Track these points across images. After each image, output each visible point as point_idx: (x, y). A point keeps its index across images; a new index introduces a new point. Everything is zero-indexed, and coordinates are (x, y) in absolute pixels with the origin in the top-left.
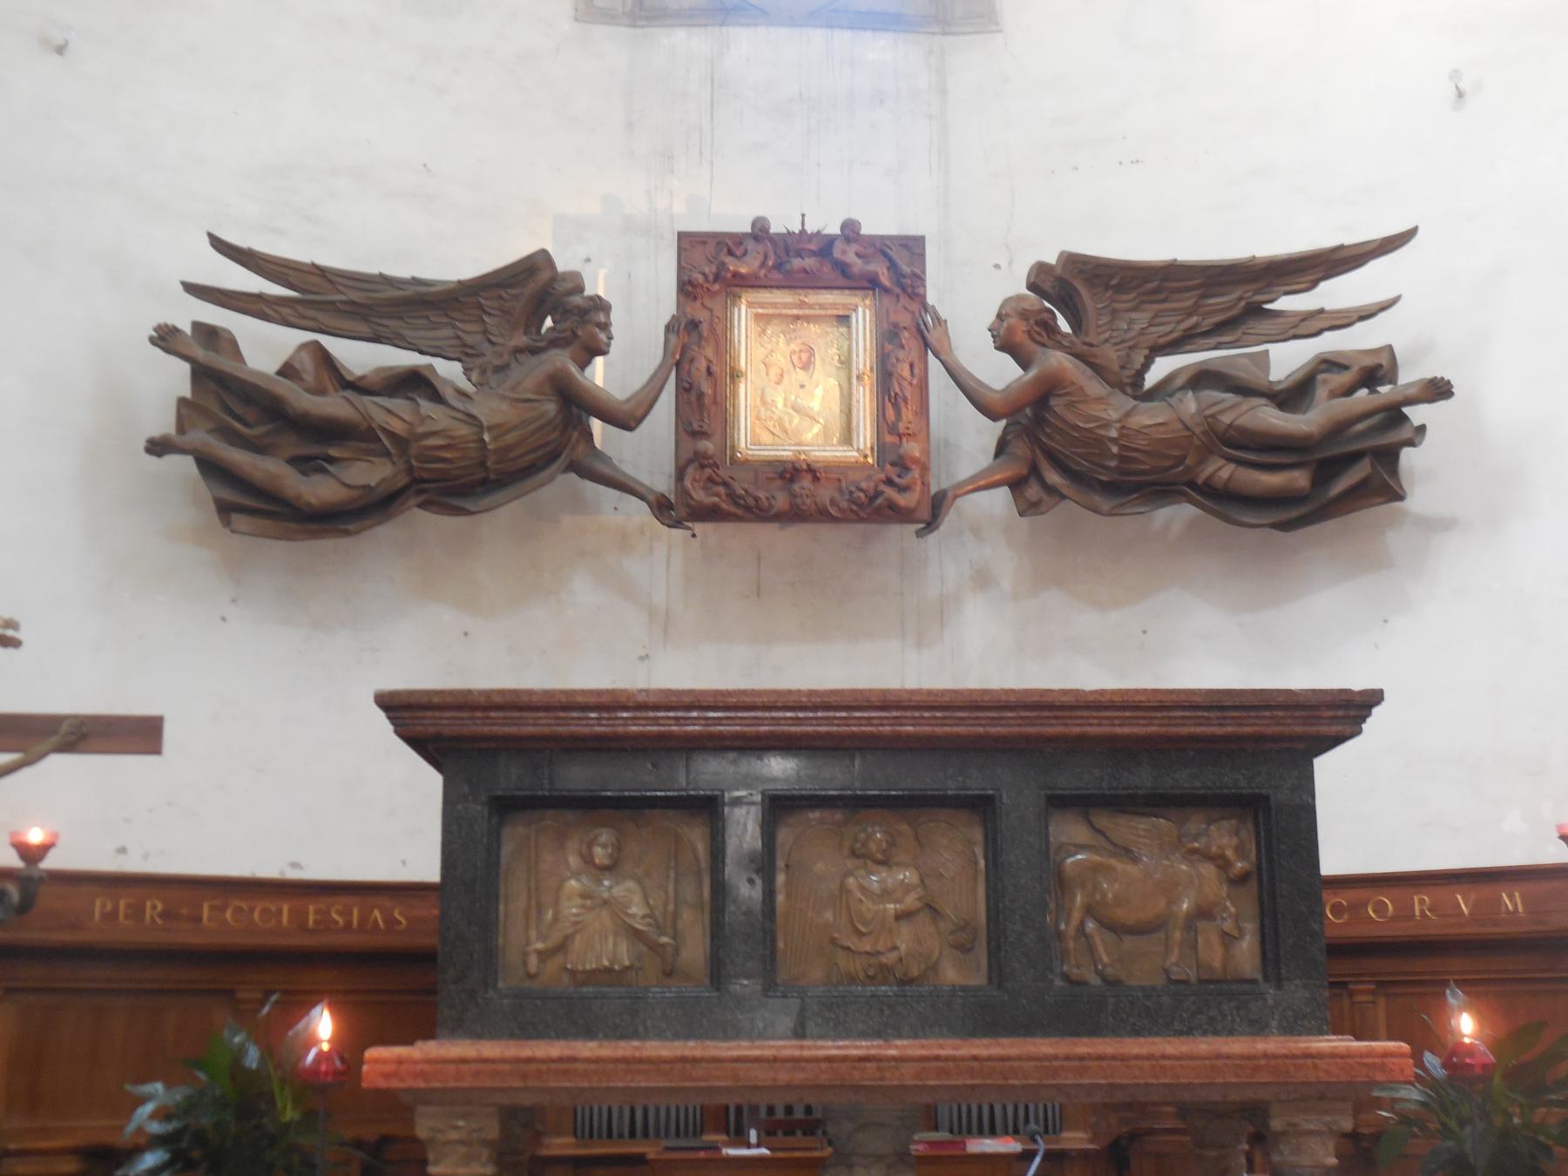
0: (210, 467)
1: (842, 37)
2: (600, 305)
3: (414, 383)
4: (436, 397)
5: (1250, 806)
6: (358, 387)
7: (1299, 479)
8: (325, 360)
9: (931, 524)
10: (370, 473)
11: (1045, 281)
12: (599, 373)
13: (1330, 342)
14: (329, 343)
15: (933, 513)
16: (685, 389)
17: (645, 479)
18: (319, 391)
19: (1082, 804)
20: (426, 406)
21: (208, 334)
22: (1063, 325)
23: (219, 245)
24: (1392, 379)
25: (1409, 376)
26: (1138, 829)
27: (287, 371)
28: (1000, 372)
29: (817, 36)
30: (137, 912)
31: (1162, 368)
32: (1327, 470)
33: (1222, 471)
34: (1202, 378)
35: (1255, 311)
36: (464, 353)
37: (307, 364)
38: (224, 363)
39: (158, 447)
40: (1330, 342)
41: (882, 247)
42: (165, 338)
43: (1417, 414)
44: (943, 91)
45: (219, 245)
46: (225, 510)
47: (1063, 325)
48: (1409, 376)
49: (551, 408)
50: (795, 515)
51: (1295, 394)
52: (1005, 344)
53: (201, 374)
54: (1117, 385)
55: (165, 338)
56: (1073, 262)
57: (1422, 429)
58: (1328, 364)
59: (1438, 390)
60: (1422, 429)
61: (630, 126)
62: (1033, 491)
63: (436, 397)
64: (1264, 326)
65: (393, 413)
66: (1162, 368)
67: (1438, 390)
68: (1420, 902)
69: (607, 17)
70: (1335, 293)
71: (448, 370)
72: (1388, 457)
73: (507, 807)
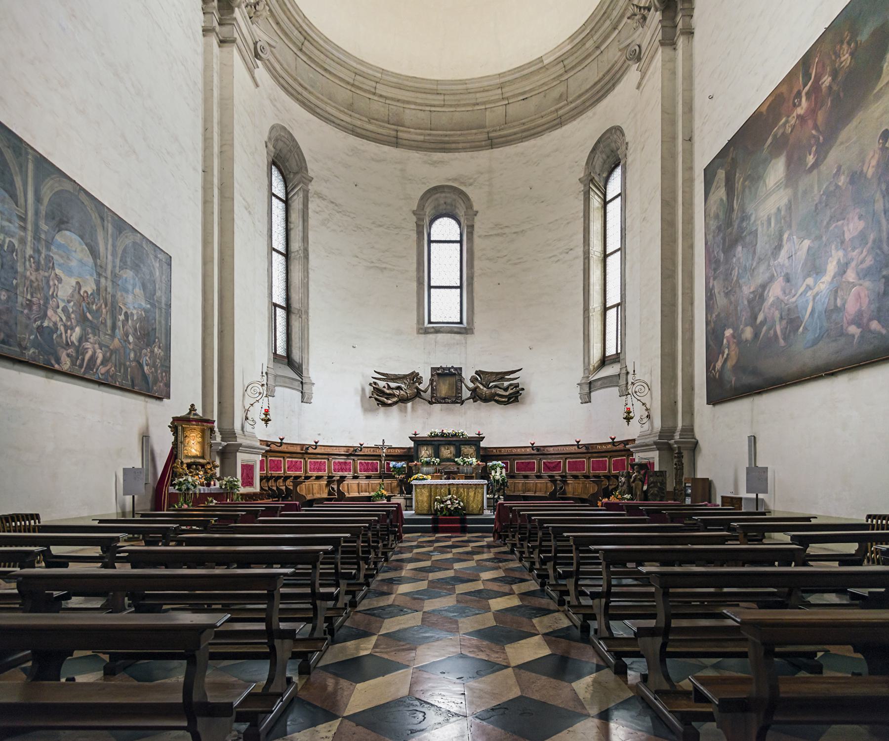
0: (376, 399)
1: (453, 335)
2: (421, 377)
3: (399, 388)
4: (402, 390)
5: (475, 445)
6: (393, 389)
7: (506, 400)
8: (388, 385)
9: (462, 404)
10: (395, 399)
11: (477, 373)
12: (421, 387)
13: (512, 382)
14: (389, 383)
15: (462, 403)
16: (432, 388)
17: (427, 398)
18: (388, 389)
19: (463, 445)
20: (401, 391)
21: (375, 383)
22: (479, 379)
23: (375, 371)
24: (518, 387)
25: (520, 387)
26: (466, 446)
27: (384, 387)
28: (471, 385)
29: (450, 334)
30: (370, 451)
31: (491, 384)
32: (509, 399)
33: (497, 398)
34: (496, 386)
35: (504, 378)
36: (405, 383)
37: (386, 386)
38: (376, 386)
39: (370, 397)
40: (512, 382)
41: (456, 369)
42: (370, 384)
43: (520, 392)
44: (466, 343)
45: (375, 371)
46: (378, 404)
47: (479, 379)
48: (520, 387)
49: (416, 390)
50: (445, 403)
51: (506, 389)
52: (472, 382)
53: (374, 388)
54: (485, 387)
55: (370, 384)
56: (480, 371)
57: (521, 394)
58: (511, 385)
59: (523, 389)
60: (521, 394)
61: (424, 349)
62: (475, 399)
63: (402, 390)
64: (504, 379)
65: (397, 392)
66: (491, 384)
67: (523, 389)
68: (519, 450)
69: (421, 334)
70: (512, 376)
71: (403, 386)
72: (517, 397)
73: (418, 445)
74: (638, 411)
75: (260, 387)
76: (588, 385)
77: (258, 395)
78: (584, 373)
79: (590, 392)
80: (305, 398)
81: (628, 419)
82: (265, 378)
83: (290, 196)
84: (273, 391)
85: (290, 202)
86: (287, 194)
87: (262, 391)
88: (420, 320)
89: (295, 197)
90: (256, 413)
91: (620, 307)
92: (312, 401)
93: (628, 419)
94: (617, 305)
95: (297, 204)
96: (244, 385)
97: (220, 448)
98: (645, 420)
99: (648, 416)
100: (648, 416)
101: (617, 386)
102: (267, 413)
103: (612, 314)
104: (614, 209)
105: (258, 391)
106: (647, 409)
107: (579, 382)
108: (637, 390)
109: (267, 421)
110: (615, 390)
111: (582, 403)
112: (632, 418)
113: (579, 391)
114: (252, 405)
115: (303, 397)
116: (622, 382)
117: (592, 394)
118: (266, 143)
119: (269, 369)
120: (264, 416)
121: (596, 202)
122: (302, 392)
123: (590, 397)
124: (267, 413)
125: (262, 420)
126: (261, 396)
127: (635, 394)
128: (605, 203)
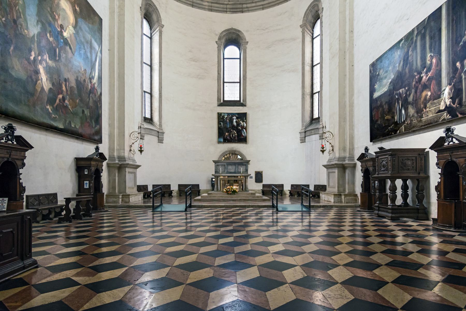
74: (328, 147)
75: (137, 134)
76: (304, 133)
77: (136, 138)
78: (302, 127)
79: (305, 137)
80: (161, 141)
81: (323, 151)
82: (140, 130)
83: (153, 34)
84: (144, 136)
85: (152, 38)
86: (151, 34)
87: (138, 137)
88: (219, 99)
89: (155, 35)
90: (136, 147)
91: (320, 93)
92: (163, 142)
93: (323, 151)
94: (319, 92)
95: (156, 38)
96: (129, 134)
97: (118, 165)
98: (331, 152)
99: (333, 150)
100: (333, 150)
101: (318, 134)
102: (141, 148)
103: (316, 97)
104: (317, 42)
105: (136, 136)
106: (332, 146)
107: (299, 132)
108: (327, 136)
109: (141, 151)
110: (317, 136)
111: (301, 143)
112: (325, 151)
113: (300, 137)
114: (133, 143)
115: (159, 140)
116: (321, 132)
117: (306, 138)
118: (141, 7)
119: (142, 125)
120: (139, 149)
121: (308, 39)
122: (158, 137)
123: (305, 140)
124: (141, 148)
125: (139, 151)
126: (138, 139)
127: (326, 139)
128: (313, 39)
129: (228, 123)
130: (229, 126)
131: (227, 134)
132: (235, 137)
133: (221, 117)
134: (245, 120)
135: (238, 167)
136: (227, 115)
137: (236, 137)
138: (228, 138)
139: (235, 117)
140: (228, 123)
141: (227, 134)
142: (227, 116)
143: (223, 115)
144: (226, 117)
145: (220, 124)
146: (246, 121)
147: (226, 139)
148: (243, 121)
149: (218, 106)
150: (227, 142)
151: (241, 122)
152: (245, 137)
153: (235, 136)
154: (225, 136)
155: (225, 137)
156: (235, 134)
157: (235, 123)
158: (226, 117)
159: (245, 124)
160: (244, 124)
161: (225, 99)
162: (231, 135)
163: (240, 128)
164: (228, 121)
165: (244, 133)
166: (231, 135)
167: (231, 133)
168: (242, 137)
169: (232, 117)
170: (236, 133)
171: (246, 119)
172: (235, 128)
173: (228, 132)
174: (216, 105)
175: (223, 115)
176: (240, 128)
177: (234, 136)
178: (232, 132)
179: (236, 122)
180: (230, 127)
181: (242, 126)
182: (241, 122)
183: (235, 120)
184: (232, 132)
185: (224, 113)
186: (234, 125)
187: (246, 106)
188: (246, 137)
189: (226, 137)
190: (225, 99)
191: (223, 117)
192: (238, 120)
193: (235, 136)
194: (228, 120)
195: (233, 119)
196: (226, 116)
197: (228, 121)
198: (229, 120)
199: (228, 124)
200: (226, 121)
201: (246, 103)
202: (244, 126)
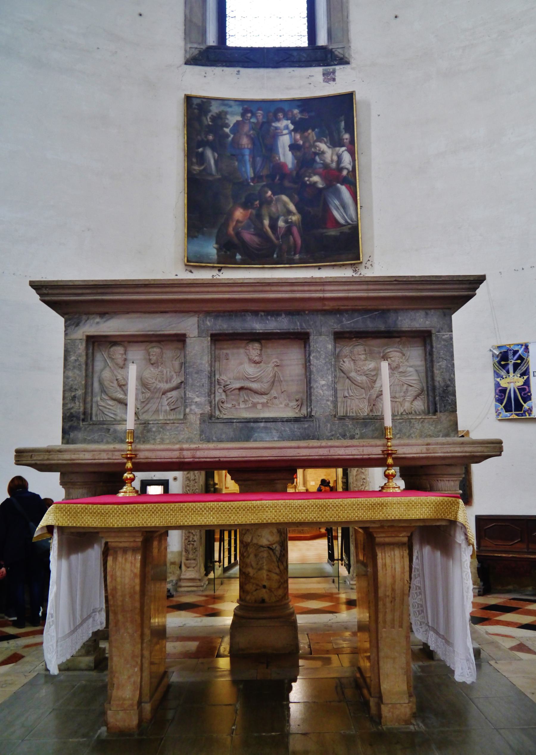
129: (247, 152)
130: (250, 173)
131: (239, 214)
132: (289, 230)
133: (207, 121)
134: (347, 136)
135: (337, 357)
136: (239, 110)
137: (295, 230)
138: (248, 236)
139: (284, 124)
140: (247, 152)
141: (239, 214)
142: (243, 115)
143: (215, 109)
144: (233, 119)
145: (201, 159)
146: (352, 141)
147: (236, 240)
148: (336, 143)
149: (186, 63)
150: (243, 262)
151: (323, 146)
152: (346, 229)
153: (290, 225)
154: (226, 224)
155: (231, 230)
156: (289, 212)
157: (289, 155)
158: (233, 119)
159: (347, 158)
160: (340, 157)
161: (231, 42)
162: (266, 222)
163: (316, 178)
164: (245, 141)
165: (344, 206)
166: (266, 222)
167: (265, 211)
168: (333, 232)
169: (268, 123)
170: (292, 207)
171: (350, 128)
172: (287, 184)
173: (245, 206)
174: (180, 57)
175: (215, 109)
176: (316, 178)
177: (281, 224)
178: (269, 202)
179: (293, 147)
180: (257, 178)
181: (326, 166)
182: (323, 146)
183: (285, 141)
184: (269, 202)
185: (223, 101)
186: (283, 166)
187: (348, 63)
188: (355, 229)
189: (238, 234)
190: (231, 42)
191: (213, 119)
192: (305, 139)
193: (290, 225)
194: (248, 136)
195: (276, 135)
196: (233, 114)
197: (245, 141)
198: (253, 140)
199: (247, 158)
200: (236, 143)
201: (347, 46)
202: (340, 169)
